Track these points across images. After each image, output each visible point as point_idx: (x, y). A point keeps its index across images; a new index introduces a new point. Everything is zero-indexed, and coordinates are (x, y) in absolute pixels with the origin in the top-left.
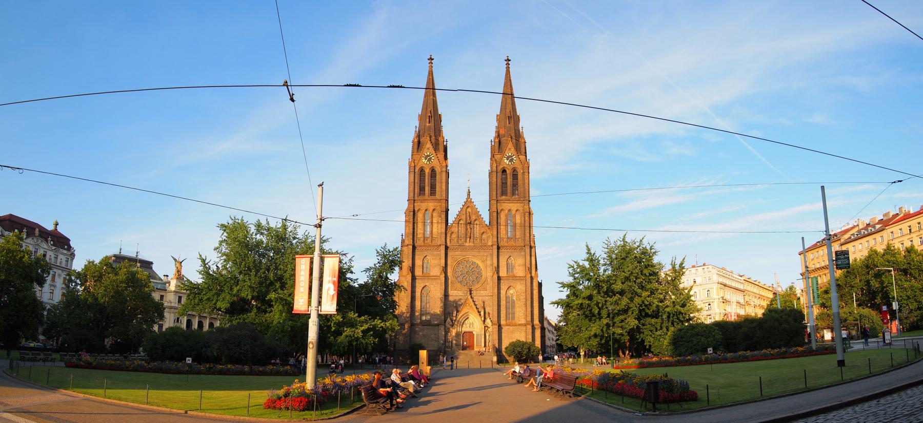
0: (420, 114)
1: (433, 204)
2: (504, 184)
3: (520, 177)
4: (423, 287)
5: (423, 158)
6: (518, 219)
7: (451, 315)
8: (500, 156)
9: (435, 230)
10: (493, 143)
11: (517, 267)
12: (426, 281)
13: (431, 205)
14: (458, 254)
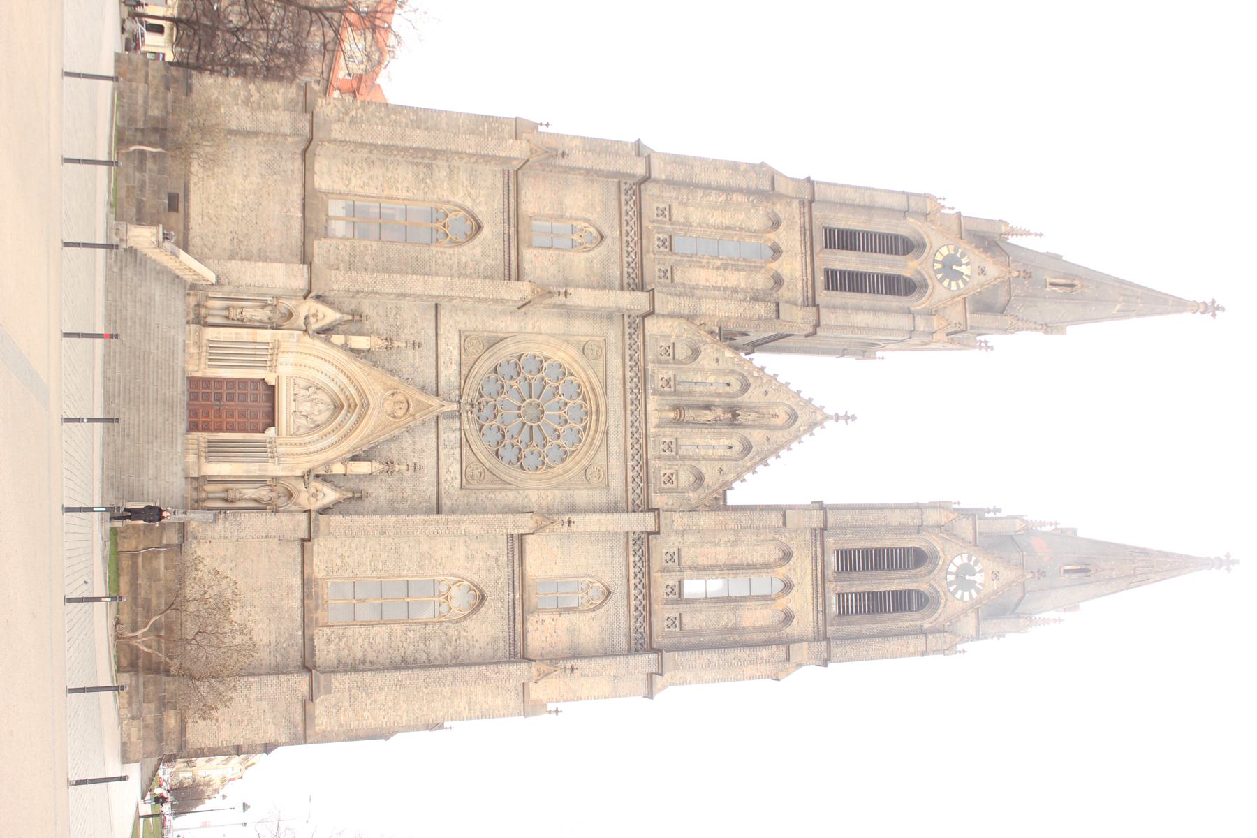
0: (1064, 258)
1: (798, 274)
2: (880, 560)
3: (907, 620)
4: (476, 211)
5: (951, 248)
6: (755, 617)
7: (353, 328)
8: (970, 537)
9: (701, 276)
10: (991, 515)
11: (564, 621)
12: (500, 228)
13: (792, 267)
14: (611, 368)
